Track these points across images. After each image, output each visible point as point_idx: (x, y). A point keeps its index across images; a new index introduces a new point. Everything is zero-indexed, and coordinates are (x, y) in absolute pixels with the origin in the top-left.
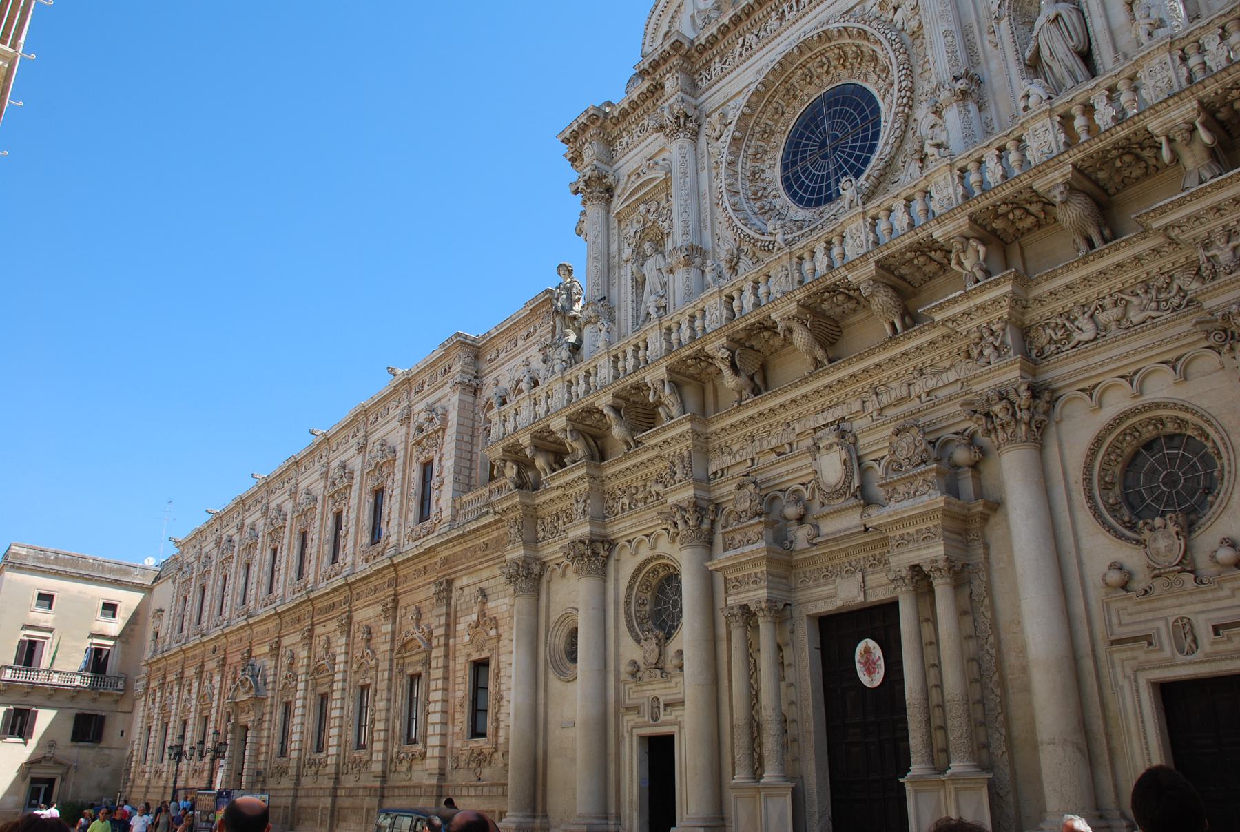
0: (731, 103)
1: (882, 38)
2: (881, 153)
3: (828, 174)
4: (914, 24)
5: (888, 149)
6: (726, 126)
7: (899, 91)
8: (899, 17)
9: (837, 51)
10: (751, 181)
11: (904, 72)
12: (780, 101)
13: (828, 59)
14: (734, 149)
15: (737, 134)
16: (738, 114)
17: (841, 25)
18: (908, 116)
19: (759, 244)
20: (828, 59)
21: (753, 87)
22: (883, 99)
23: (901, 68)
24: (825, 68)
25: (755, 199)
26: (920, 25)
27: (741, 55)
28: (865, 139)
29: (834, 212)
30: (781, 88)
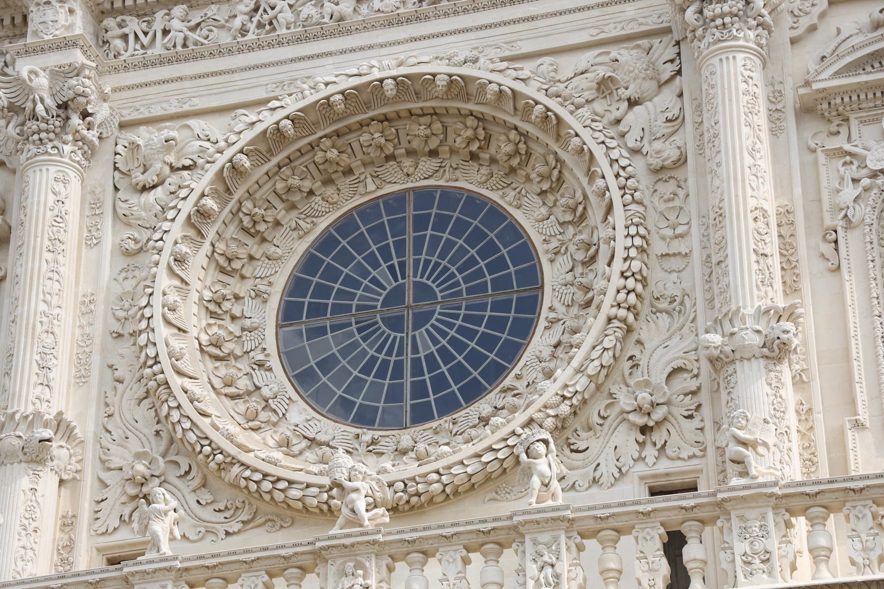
0: (197, 124)
1: (599, 152)
2: (566, 386)
3: (399, 365)
4: (670, 153)
5: (582, 383)
6: (173, 169)
7: (622, 273)
8: (636, 118)
9: (470, 121)
10: (213, 314)
11: (638, 241)
12: (312, 167)
13: (445, 128)
14: (192, 233)
15: (210, 203)
16: (221, 160)
17: (508, 82)
18: (629, 330)
19: (236, 469)
20: (445, 128)
21: (268, 120)
22: (552, 261)
23: (633, 230)
24: (434, 143)
25: (217, 358)
26: (681, 161)
27: (243, 31)
28: (497, 324)
29: (439, 465)
30: (327, 143)
